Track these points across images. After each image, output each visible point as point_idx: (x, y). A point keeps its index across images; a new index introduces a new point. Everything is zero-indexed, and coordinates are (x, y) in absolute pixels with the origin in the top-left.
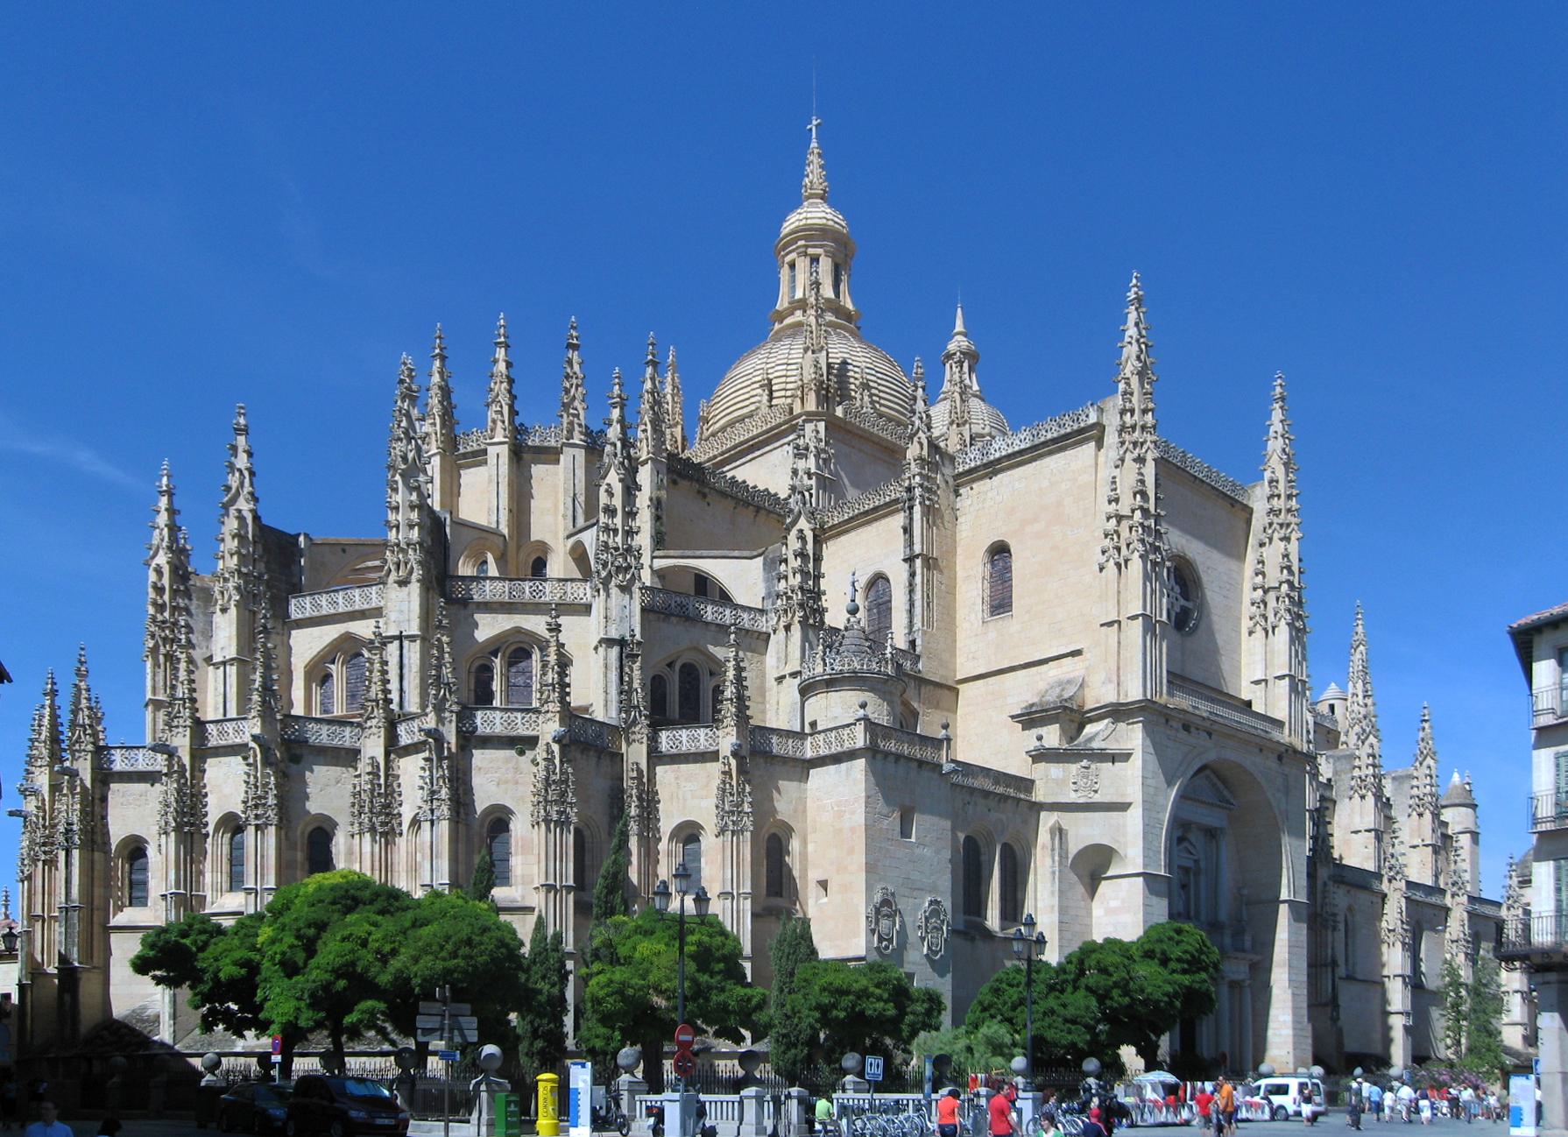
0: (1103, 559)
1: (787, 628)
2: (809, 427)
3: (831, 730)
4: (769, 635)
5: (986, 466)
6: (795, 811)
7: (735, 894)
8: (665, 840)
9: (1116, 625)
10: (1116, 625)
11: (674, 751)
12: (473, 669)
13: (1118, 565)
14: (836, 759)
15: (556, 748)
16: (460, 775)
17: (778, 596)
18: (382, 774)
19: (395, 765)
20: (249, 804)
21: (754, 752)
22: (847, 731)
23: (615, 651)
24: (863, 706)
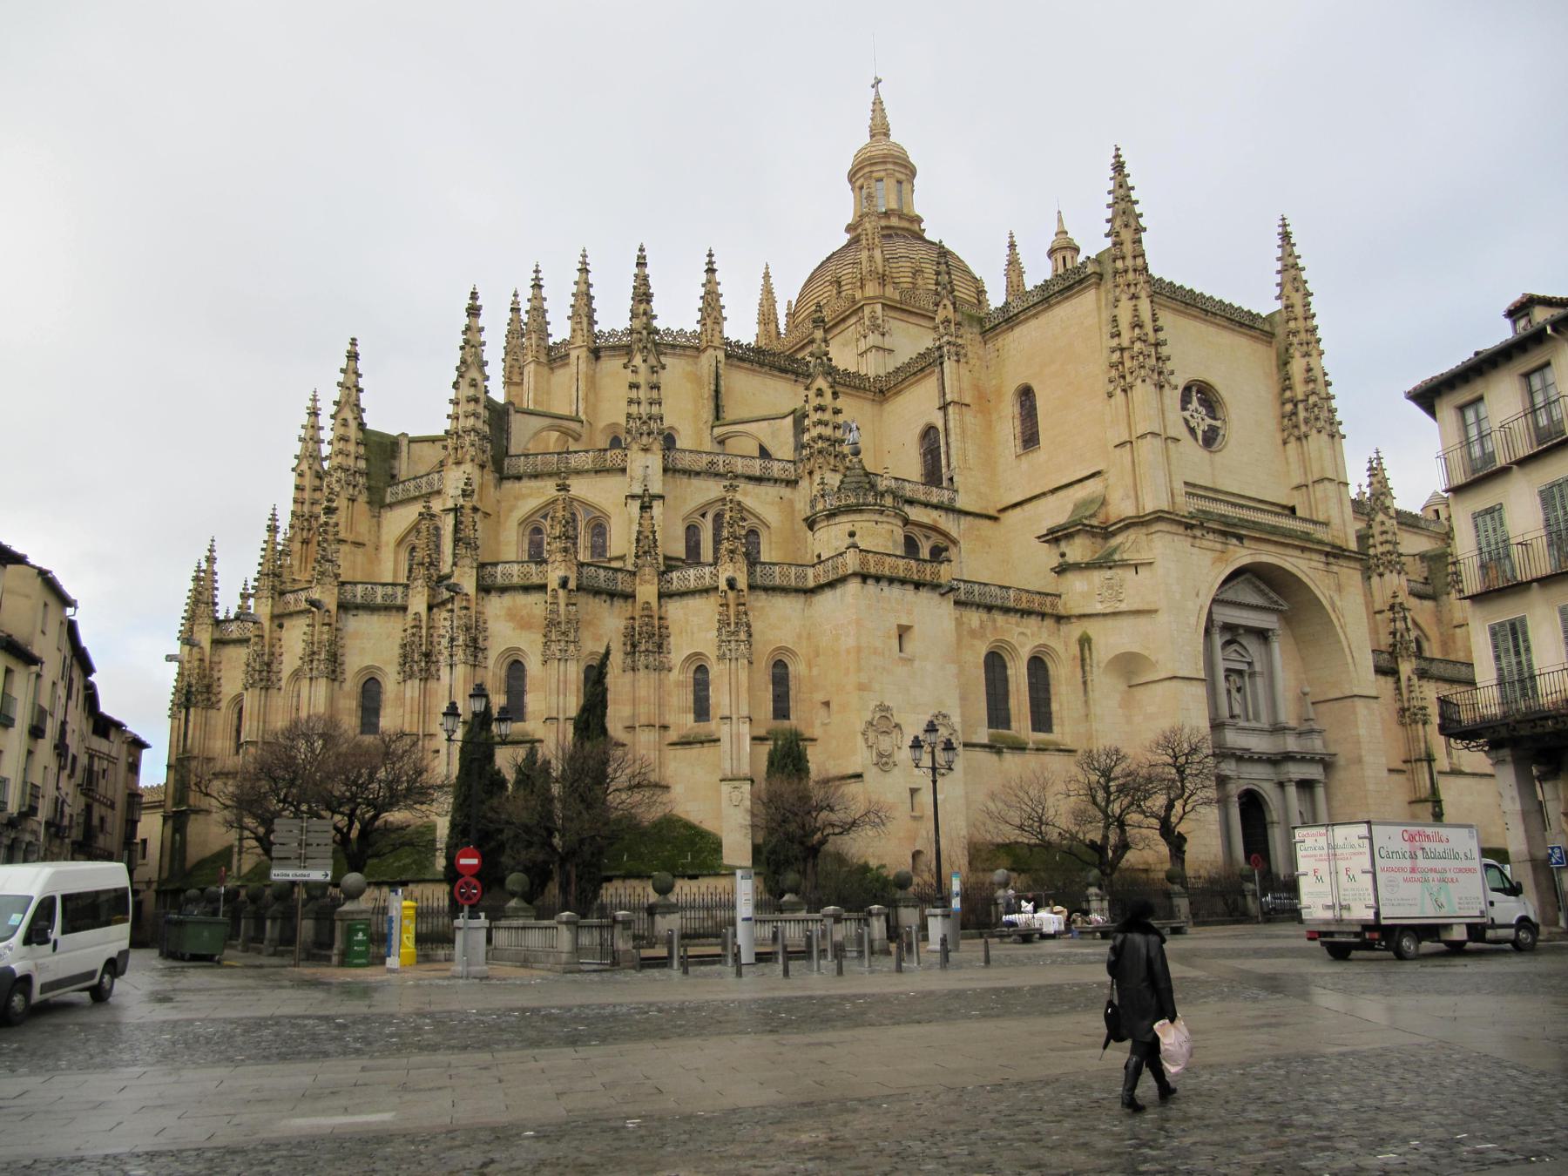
0: (1111, 387)
1: (811, 473)
2: (867, 310)
3: (828, 559)
4: (796, 482)
5: (1006, 321)
6: (800, 636)
7: (734, 717)
8: (675, 671)
9: (1128, 445)
10: (1128, 445)
11: (683, 589)
12: (527, 533)
13: (1124, 391)
14: (831, 585)
15: (561, 593)
16: (481, 623)
17: (803, 447)
18: (424, 624)
19: (436, 617)
20: (307, 659)
21: (752, 587)
22: (840, 559)
23: (638, 503)
24: (852, 534)
